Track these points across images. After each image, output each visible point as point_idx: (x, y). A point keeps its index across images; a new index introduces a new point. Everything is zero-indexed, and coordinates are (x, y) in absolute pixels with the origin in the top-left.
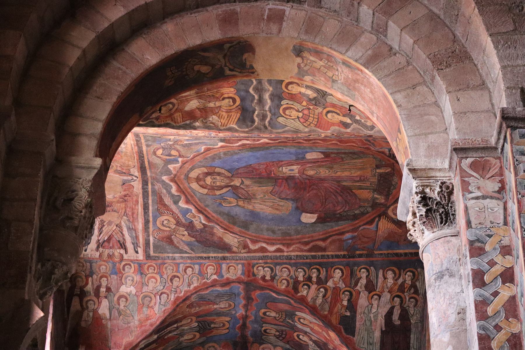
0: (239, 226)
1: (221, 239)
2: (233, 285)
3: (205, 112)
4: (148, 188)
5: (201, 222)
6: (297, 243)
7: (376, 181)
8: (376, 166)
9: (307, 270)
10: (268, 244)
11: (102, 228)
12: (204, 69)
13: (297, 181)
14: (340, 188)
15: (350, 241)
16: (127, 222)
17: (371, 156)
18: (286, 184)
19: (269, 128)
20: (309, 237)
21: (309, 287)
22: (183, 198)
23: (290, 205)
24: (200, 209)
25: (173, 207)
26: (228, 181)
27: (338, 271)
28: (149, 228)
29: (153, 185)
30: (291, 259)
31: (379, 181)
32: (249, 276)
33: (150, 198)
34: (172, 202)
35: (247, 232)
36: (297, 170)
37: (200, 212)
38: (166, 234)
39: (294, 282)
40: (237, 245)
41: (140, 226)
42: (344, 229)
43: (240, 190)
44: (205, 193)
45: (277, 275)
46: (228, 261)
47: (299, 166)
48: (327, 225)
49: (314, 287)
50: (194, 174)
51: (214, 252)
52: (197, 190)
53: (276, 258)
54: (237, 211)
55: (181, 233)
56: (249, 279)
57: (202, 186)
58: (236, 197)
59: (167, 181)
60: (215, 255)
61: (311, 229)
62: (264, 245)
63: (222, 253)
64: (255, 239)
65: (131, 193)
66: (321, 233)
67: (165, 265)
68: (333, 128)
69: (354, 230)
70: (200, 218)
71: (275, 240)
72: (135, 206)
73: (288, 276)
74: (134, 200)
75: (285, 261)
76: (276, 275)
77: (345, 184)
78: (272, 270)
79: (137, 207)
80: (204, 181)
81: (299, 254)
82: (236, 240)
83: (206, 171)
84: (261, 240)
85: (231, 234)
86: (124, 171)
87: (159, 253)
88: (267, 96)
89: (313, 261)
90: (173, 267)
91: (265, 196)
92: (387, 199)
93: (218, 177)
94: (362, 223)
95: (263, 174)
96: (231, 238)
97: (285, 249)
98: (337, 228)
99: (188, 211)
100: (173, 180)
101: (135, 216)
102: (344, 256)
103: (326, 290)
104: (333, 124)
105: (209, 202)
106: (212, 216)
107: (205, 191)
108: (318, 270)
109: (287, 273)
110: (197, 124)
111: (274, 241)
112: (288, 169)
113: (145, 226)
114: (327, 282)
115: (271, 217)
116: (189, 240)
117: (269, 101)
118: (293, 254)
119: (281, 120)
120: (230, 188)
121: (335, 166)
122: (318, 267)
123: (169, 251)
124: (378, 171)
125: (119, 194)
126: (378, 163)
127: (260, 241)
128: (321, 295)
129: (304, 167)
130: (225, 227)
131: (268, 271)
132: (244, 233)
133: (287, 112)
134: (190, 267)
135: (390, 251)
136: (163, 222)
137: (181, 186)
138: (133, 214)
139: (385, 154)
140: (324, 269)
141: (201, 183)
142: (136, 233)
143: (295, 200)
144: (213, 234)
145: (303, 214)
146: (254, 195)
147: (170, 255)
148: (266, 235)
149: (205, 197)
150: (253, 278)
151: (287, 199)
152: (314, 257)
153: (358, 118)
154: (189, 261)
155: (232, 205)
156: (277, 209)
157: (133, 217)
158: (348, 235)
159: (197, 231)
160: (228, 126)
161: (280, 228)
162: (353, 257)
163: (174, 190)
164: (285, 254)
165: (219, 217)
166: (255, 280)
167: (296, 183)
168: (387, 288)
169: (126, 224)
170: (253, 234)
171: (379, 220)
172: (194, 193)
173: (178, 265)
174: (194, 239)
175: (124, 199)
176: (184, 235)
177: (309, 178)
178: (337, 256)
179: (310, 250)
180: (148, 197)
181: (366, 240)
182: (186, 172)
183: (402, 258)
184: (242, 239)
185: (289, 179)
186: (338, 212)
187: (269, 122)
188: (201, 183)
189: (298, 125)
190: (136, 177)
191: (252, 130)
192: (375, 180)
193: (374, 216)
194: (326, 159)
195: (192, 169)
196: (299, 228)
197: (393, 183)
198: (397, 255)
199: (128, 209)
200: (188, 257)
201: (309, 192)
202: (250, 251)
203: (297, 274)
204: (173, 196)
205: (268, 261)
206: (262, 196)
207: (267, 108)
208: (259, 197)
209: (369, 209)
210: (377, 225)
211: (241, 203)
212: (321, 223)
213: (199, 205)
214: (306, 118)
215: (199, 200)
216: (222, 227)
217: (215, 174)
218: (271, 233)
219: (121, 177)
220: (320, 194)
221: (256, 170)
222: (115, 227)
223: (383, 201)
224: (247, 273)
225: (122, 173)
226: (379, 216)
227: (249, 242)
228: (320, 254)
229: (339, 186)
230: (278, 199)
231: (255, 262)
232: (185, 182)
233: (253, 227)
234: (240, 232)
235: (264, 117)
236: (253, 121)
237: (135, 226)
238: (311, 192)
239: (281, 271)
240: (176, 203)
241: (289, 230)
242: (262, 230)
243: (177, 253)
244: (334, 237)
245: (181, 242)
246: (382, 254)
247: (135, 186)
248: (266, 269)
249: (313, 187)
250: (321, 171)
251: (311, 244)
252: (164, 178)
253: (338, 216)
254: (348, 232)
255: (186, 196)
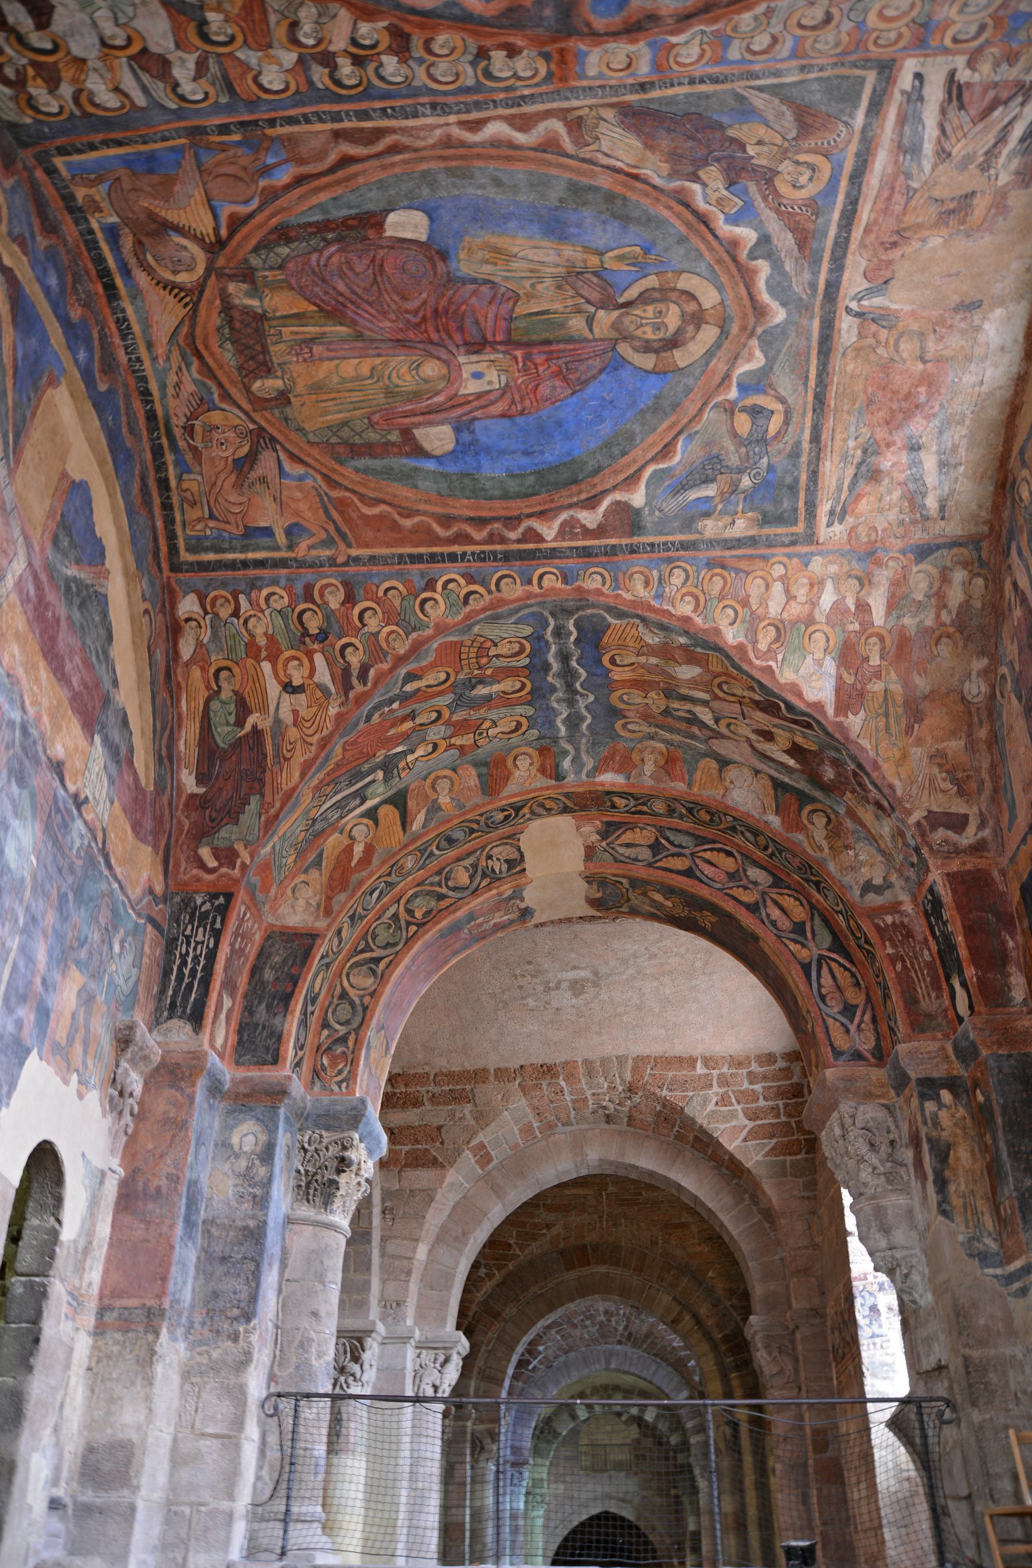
0: (595, 189)
1: (649, 147)
2: (617, 20)
3: (665, 652)
4: (831, 271)
5: (705, 185)
6: (425, 148)
7: (272, 348)
8: (289, 402)
9: (376, 82)
10: (511, 145)
11: (995, 145)
12: (658, 897)
13: (458, 337)
14: (350, 314)
15: (270, 161)
16: (915, 172)
17: (311, 437)
18: (482, 324)
19: (546, 613)
20: (393, 165)
21: (354, 42)
22: (743, 255)
23: (464, 265)
24: (703, 228)
25: (774, 225)
26: (627, 320)
27: (277, 86)
28: (858, 155)
29: (813, 286)
30: (434, 106)
31: (265, 351)
32: (562, 51)
33: (829, 243)
34: (775, 241)
35: (574, 177)
36: (465, 375)
37: (704, 220)
38: (811, 143)
39: (408, 50)
40: (603, 127)
41: (881, 162)
42: (302, 197)
43: (595, 296)
44: (685, 275)
45: (471, 63)
46: (631, 81)
47: (462, 392)
48: (350, 208)
49: (339, 43)
50: (709, 334)
51: (670, 101)
52: (706, 283)
53: (478, 106)
54: (601, 235)
55: (766, 149)
56: (559, 45)
57: (691, 296)
58: (604, 274)
59: (774, 305)
60: (670, 92)
61: (392, 192)
62: (520, 138)
63: (649, 100)
64: (548, 156)
65: (875, 255)
66: (361, 180)
67: (838, 50)
68: (430, 658)
69: (271, 195)
70: (705, 196)
71: (491, 157)
72: (876, 221)
73: (433, 64)
74: (873, 236)
75: (450, 99)
76: (473, 64)
77: (343, 330)
78: (488, 74)
79: (873, 216)
80: (683, 314)
81: (411, 123)
82: (605, 145)
83: (677, 353)
84: (531, 154)
85: (619, 164)
86: (874, 327)
87: (847, 78)
88: (556, 666)
89: (364, 105)
90: (813, 47)
91: (533, 286)
92: (224, 296)
93: (650, 336)
94: (259, 218)
95: (544, 357)
96: (620, 153)
97: (457, 132)
98: (323, 197)
99: (734, 220)
100: (760, 311)
101: (886, 194)
102: (272, 123)
103: (295, 42)
104: (433, 666)
105: (676, 256)
106: (669, 208)
107: (685, 283)
108: (338, 83)
109: (437, 72)
110: (683, 640)
111: (494, 152)
112: (487, 378)
113: (866, 161)
114: (301, 60)
115: (512, 224)
116: (745, 127)
117: (551, 660)
118: (430, 120)
119: (528, 631)
120: (621, 300)
121: (381, 399)
122: (343, 92)
123: (815, 86)
124: (279, 384)
125: (908, 250)
126: (288, 410)
127: (534, 149)
128: (307, 27)
129: (451, 391)
130: (639, 185)
131: (501, 70)
132: (584, 173)
133: (516, 647)
134: (755, 53)
135: (143, 148)
136: (811, 179)
137: (743, 292)
138: (889, 199)
139: (286, 450)
140: (320, 86)
141: (691, 307)
142: (901, 135)
143: (452, 280)
144: (674, 157)
145: (423, 238)
146: (559, 287)
147: (813, 75)
148: (519, 173)
149: (686, 265)
150: (547, 49)
151: (474, 281)
152: (364, 115)
153: (395, 705)
154: (756, 67)
155: (615, 253)
156: (496, 250)
157: (893, 188)
158: (283, 176)
159: (718, 160)
160: (625, 622)
161: (479, 192)
162: (242, 124)
163: (763, 269)
164: (453, 118)
165: (652, 211)
166: (543, 44)
167: (461, 329)
168: (95, 70)
169: (919, 165)
170: (554, 172)
171: (216, 230)
172: (713, 271)
173: (795, 54)
174: (731, 133)
175: (900, 236)
176: (760, 143)
177: (429, 347)
178: (291, 121)
179: (379, 133)
180: (836, 243)
181: (230, 170)
182: (726, 344)
183: (99, 137)
184: (586, 152)
185: (477, 346)
186: (333, 249)
187: (548, 625)
188: (691, 307)
189: (492, 632)
190: (848, 311)
191: (578, 609)
192: (278, 351)
193: (234, 242)
194: (407, 421)
195: (710, 354)
196: (426, 192)
197: (228, 345)
198: (119, 143)
199: (898, 208)
200: (758, 78)
201: (424, 303)
202: (562, 114)
203: (404, 70)
204: (769, 256)
205: (502, 96)
206: (539, 287)
207: (553, 648)
208: (548, 282)
209: (255, 261)
210: (215, 217)
211: (594, 261)
212: (371, 214)
213: (704, 239)
214: (482, 651)
215: (701, 256)
216: (646, 182)
217: (655, 345)
218: (505, 178)
219: (887, 303)
220: (396, 298)
221: (558, 374)
222: (954, 152)
223: (232, 288)
224: (570, 58)
225: (882, 317)
226: (220, 244)
227: (568, 145)
228: (347, 124)
229: (354, 323)
230: (497, 280)
231: (543, 89)
232: (732, 310)
233: (555, 194)
234: (593, 175)
235: (559, 632)
236: (577, 625)
237: (896, 162)
238: (417, 303)
239: (457, 75)
240: (765, 240)
241: (454, 185)
242: (532, 185)
243: (790, 84)
244: (320, 167)
245: (771, 117)
246: (165, 139)
247: (859, 278)
248: (507, 74)
249: (417, 320)
250: (408, 378)
251: (380, 146)
252: (779, 315)
253: (330, 236)
254: (288, 188)
255: (735, 259)
